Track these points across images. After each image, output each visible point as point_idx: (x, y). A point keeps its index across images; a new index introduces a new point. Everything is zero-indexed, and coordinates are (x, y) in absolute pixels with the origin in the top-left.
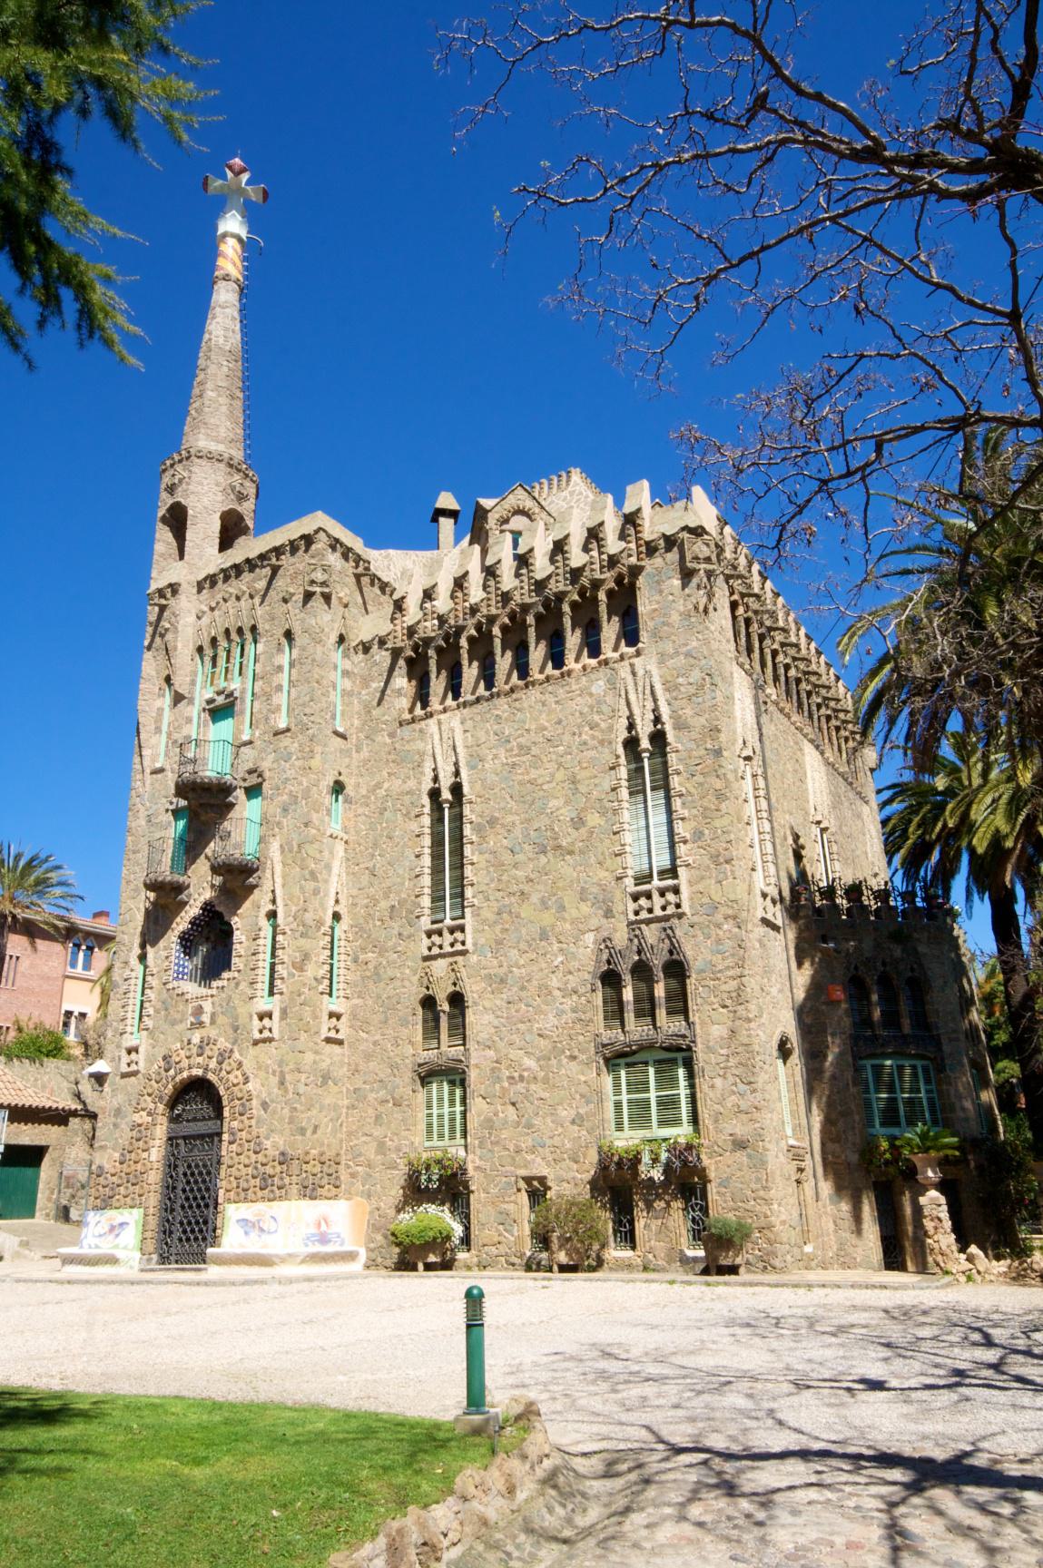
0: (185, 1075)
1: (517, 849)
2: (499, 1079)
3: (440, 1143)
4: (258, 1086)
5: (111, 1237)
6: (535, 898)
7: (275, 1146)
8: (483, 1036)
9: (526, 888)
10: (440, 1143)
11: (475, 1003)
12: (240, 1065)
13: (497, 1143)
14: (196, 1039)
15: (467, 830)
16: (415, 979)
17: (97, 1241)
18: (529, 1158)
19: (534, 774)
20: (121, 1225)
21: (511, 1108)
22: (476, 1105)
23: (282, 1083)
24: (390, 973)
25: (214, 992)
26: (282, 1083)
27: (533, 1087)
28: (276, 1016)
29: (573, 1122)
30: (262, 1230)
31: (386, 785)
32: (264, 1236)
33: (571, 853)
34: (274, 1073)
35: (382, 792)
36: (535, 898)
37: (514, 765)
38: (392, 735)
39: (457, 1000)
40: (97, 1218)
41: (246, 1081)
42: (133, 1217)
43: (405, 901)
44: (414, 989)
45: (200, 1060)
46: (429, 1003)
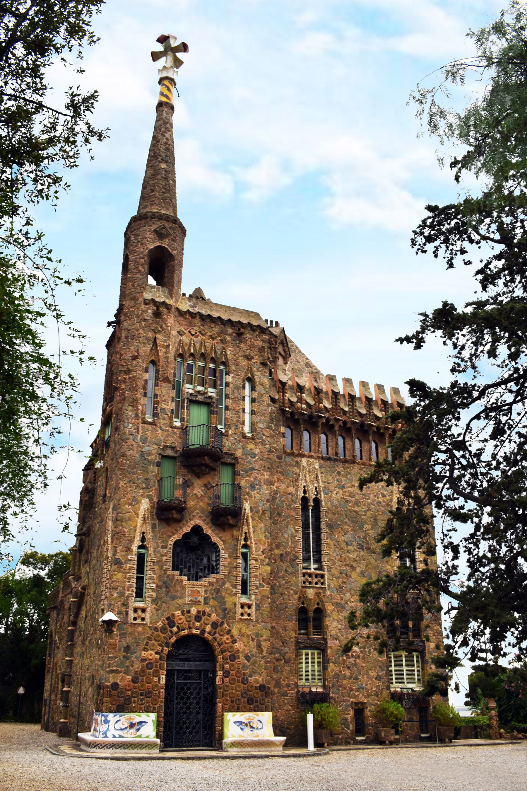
0: (186, 632)
1: (349, 543)
3: (307, 684)
4: (242, 646)
5: (133, 731)
6: (358, 570)
7: (256, 681)
8: (333, 633)
9: (354, 564)
10: (307, 684)
11: (329, 616)
12: (229, 632)
13: (341, 686)
14: (194, 611)
15: (323, 526)
16: (296, 597)
17: (121, 733)
18: (357, 693)
19: (356, 508)
20: (140, 723)
21: (346, 669)
22: (331, 666)
23: (259, 646)
24: (281, 589)
25: (206, 584)
26: (259, 646)
27: (358, 661)
28: (253, 607)
29: (376, 679)
30: (252, 727)
31: (276, 484)
32: (255, 731)
33: (374, 553)
34: (253, 640)
35: (274, 488)
36: (358, 570)
37: (347, 501)
38: (279, 457)
39: (320, 612)
40: (117, 718)
41: (234, 641)
42: (151, 718)
43: (289, 553)
44: (295, 602)
45: (197, 624)
46: (302, 612)
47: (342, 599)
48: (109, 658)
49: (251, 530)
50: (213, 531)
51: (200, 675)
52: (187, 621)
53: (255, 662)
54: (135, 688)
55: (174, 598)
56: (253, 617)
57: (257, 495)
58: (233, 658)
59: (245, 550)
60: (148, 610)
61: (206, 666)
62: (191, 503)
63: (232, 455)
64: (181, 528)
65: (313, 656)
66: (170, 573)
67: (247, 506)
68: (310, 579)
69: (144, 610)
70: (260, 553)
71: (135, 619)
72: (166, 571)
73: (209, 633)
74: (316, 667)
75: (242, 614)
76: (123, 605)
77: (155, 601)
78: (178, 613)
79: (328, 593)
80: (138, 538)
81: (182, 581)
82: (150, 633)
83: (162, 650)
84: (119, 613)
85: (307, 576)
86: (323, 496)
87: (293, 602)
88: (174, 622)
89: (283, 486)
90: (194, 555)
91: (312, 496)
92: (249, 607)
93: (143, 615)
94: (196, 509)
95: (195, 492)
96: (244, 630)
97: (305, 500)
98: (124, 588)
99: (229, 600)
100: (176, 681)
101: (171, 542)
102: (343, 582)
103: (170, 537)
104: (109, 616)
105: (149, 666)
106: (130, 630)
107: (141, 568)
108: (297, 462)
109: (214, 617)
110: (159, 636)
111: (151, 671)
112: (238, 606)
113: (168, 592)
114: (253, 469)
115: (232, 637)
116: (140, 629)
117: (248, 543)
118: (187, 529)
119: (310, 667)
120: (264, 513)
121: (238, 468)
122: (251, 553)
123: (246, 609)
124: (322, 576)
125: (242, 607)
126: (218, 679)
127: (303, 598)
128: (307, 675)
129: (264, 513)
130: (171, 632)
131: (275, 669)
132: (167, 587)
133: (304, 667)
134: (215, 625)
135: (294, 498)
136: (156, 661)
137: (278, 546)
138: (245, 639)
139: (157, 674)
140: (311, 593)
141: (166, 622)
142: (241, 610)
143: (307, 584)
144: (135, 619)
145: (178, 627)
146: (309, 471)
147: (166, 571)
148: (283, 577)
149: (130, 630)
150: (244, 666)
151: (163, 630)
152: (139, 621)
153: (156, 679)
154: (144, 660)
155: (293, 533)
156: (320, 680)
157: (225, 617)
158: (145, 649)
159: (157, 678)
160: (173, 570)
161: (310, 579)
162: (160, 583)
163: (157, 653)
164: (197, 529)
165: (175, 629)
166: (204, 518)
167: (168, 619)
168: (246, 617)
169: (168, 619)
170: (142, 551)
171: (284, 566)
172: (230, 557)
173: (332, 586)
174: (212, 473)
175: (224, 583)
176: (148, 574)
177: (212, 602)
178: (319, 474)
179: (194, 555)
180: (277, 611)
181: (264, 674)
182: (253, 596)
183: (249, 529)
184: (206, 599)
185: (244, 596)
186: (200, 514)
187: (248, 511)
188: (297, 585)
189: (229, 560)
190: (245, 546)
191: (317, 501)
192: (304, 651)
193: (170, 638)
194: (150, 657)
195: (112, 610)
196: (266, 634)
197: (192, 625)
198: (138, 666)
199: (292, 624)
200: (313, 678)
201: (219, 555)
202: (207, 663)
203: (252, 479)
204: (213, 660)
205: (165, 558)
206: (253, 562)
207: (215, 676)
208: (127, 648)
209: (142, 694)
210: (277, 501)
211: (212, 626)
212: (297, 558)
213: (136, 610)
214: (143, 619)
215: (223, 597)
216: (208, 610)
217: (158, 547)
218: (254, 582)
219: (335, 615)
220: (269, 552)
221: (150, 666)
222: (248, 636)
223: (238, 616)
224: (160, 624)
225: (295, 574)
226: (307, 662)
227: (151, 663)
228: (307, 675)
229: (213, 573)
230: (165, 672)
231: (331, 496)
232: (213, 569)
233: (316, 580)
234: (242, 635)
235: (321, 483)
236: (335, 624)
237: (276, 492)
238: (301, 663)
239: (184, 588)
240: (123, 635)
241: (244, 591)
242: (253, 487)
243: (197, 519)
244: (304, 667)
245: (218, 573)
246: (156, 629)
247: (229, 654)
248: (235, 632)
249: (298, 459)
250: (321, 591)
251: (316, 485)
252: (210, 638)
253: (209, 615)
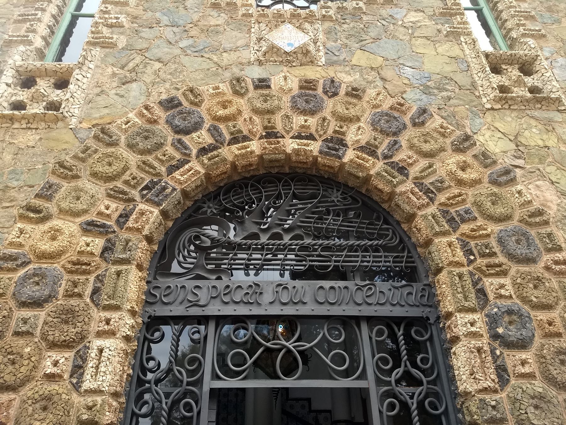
0: (255, 146)
41: (504, 178)
51: (351, 345)
52: (256, 111)
73: (369, 149)
83: (125, 216)
100: (209, 383)
105: (31, 291)
111: (42, 315)
136: (79, 267)
141: (160, 114)
145: (214, 131)
159: (65, 359)
163: (90, 228)
169: (170, 104)
193: (171, 170)
194: (47, 246)
197: (279, 127)
202: (380, 284)
204: (410, 267)
211: (374, 124)
230: (126, 323)
247: (492, 228)
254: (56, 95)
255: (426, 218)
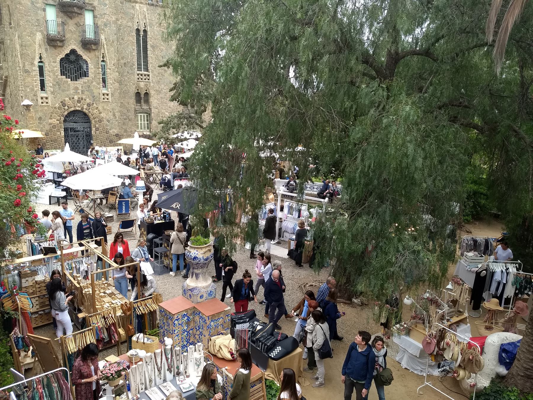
0: (73, 109)
2: (159, 117)
4: (105, 115)
7: (114, 132)
8: (155, 105)
14: (76, 98)
15: (149, 47)
16: (134, 87)
23: (114, 115)
26: (114, 115)
28: (110, 95)
34: (111, 112)
35: (119, 23)
39: (147, 94)
41: (100, 113)
44: (134, 89)
45: (79, 105)
46: (138, 94)
47: (159, 88)
48: (30, 124)
49: (106, 52)
50: (83, 52)
53: (112, 123)
54: (47, 138)
55: (63, 91)
56: (110, 100)
57: (109, 31)
58: (100, 121)
59: (103, 63)
60: (49, 98)
61: (86, 125)
62: (68, 36)
63: (91, 4)
64: (63, 51)
65: (144, 116)
66: (60, 77)
67: (103, 37)
68: (141, 77)
69: (47, 98)
70: (112, 65)
71: (42, 103)
72: (57, 76)
74: (146, 122)
75: (104, 99)
76: (34, 95)
77: (52, 93)
78: (67, 99)
79: (152, 84)
80: (37, 57)
81: (67, 82)
82: (52, 110)
84: (32, 100)
85: (140, 75)
86: (148, 29)
87: (133, 90)
88: (65, 104)
89: (125, 22)
90: (73, 66)
91: (142, 29)
92: (108, 95)
93: (47, 101)
94: (71, 39)
95: (69, 28)
96: (105, 107)
97: (138, 30)
98: (33, 86)
99: (96, 92)
101: (58, 60)
102: (160, 79)
103: (57, 56)
104: (26, 102)
106: (40, 109)
107: (41, 74)
108: (133, 6)
109: (88, 101)
110: (57, 111)
112: (101, 95)
113: (59, 88)
114: (105, 14)
115: (99, 110)
116: (46, 108)
117: (105, 59)
118: (67, 51)
119: (143, 122)
120: (113, 42)
121: (96, 13)
122: (107, 65)
123: (106, 96)
124: (148, 75)
125: (103, 95)
126: (93, 131)
127: (138, 87)
128: (141, 126)
129: (113, 42)
130: (64, 109)
131: (124, 124)
132: (59, 85)
133: (139, 122)
134: (89, 105)
135: (131, 29)
136: (58, 124)
137: (123, 58)
138: (106, 112)
139: (58, 130)
140: (142, 85)
142: (103, 97)
143: (140, 80)
144: (42, 103)
145: (68, 106)
146: (140, 12)
147: (57, 76)
148: (126, 76)
149: (40, 109)
150: (106, 125)
151: (59, 108)
152: (45, 104)
153: (59, 133)
154: (50, 124)
155: (131, 50)
156: (148, 128)
157: (94, 101)
158: (50, 118)
160: (61, 75)
161: (141, 77)
162: (55, 83)
163: (57, 120)
164: (73, 52)
165: (66, 108)
166: (77, 44)
167: (61, 102)
168: (106, 100)
169: (61, 102)
170: (41, 64)
171: (127, 69)
172: (95, 68)
173: (154, 80)
174: (80, 16)
175: (92, 82)
176: (47, 78)
177: (86, 93)
178: (146, 14)
179: (73, 66)
180: (123, 94)
181: (118, 129)
182: (109, 89)
183: (105, 51)
184: (82, 91)
185: (104, 89)
186: (75, 42)
187: (104, 41)
188: (134, 81)
189: (94, 69)
190: (103, 61)
191: (145, 31)
192: (139, 115)
195: (28, 99)
196: (117, 109)
198: (47, 127)
199: (133, 100)
200: (145, 127)
201: (88, 67)
203: (105, 20)
205: (55, 68)
206: (108, 70)
207: (91, 130)
208: (40, 118)
209: (52, 141)
210: (121, 31)
212: (134, 65)
213: (42, 98)
214: (47, 103)
215: (92, 90)
216: (84, 97)
217: (51, 62)
218: (109, 81)
219: (156, 96)
220: (118, 65)
221: (54, 127)
222: (108, 110)
223: (102, 100)
224: (57, 105)
225: (133, 74)
226: (141, 120)
227: (55, 126)
228: (141, 126)
229: (85, 76)
231: (153, 29)
232: (86, 74)
233: (145, 77)
234: (104, 109)
235: (148, 20)
236: (156, 101)
237: (120, 26)
238: (138, 121)
239: (69, 85)
240: (36, 112)
241: (105, 86)
242: (105, 25)
243: (73, 45)
244: (139, 122)
245: (88, 76)
246: (55, 108)
248: (100, 108)
249: (134, 4)
250: (148, 83)
251: (144, 21)
252: (87, 112)
253: (85, 100)
254: (47, 101)
255: (91, 118)
